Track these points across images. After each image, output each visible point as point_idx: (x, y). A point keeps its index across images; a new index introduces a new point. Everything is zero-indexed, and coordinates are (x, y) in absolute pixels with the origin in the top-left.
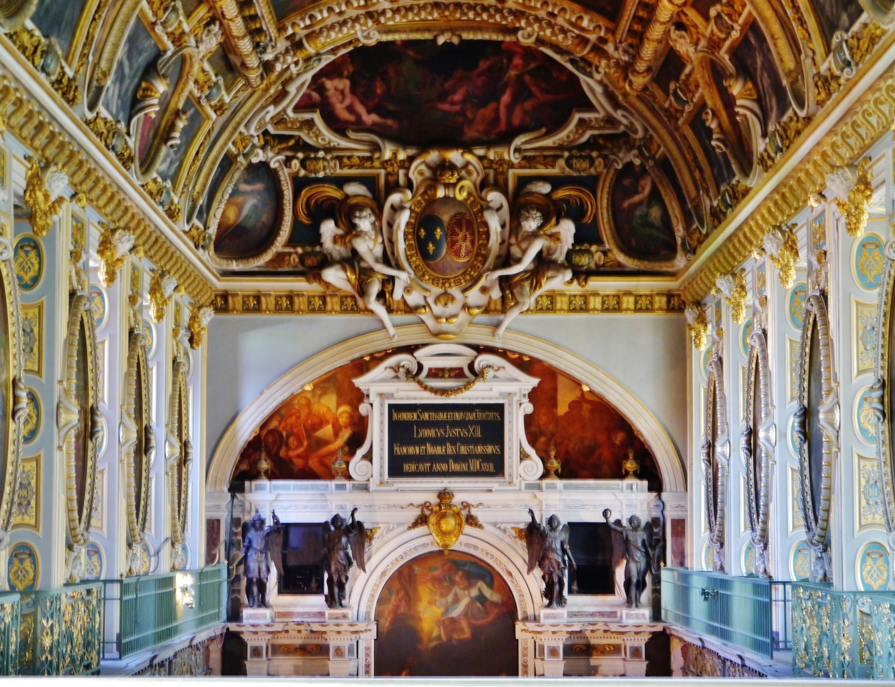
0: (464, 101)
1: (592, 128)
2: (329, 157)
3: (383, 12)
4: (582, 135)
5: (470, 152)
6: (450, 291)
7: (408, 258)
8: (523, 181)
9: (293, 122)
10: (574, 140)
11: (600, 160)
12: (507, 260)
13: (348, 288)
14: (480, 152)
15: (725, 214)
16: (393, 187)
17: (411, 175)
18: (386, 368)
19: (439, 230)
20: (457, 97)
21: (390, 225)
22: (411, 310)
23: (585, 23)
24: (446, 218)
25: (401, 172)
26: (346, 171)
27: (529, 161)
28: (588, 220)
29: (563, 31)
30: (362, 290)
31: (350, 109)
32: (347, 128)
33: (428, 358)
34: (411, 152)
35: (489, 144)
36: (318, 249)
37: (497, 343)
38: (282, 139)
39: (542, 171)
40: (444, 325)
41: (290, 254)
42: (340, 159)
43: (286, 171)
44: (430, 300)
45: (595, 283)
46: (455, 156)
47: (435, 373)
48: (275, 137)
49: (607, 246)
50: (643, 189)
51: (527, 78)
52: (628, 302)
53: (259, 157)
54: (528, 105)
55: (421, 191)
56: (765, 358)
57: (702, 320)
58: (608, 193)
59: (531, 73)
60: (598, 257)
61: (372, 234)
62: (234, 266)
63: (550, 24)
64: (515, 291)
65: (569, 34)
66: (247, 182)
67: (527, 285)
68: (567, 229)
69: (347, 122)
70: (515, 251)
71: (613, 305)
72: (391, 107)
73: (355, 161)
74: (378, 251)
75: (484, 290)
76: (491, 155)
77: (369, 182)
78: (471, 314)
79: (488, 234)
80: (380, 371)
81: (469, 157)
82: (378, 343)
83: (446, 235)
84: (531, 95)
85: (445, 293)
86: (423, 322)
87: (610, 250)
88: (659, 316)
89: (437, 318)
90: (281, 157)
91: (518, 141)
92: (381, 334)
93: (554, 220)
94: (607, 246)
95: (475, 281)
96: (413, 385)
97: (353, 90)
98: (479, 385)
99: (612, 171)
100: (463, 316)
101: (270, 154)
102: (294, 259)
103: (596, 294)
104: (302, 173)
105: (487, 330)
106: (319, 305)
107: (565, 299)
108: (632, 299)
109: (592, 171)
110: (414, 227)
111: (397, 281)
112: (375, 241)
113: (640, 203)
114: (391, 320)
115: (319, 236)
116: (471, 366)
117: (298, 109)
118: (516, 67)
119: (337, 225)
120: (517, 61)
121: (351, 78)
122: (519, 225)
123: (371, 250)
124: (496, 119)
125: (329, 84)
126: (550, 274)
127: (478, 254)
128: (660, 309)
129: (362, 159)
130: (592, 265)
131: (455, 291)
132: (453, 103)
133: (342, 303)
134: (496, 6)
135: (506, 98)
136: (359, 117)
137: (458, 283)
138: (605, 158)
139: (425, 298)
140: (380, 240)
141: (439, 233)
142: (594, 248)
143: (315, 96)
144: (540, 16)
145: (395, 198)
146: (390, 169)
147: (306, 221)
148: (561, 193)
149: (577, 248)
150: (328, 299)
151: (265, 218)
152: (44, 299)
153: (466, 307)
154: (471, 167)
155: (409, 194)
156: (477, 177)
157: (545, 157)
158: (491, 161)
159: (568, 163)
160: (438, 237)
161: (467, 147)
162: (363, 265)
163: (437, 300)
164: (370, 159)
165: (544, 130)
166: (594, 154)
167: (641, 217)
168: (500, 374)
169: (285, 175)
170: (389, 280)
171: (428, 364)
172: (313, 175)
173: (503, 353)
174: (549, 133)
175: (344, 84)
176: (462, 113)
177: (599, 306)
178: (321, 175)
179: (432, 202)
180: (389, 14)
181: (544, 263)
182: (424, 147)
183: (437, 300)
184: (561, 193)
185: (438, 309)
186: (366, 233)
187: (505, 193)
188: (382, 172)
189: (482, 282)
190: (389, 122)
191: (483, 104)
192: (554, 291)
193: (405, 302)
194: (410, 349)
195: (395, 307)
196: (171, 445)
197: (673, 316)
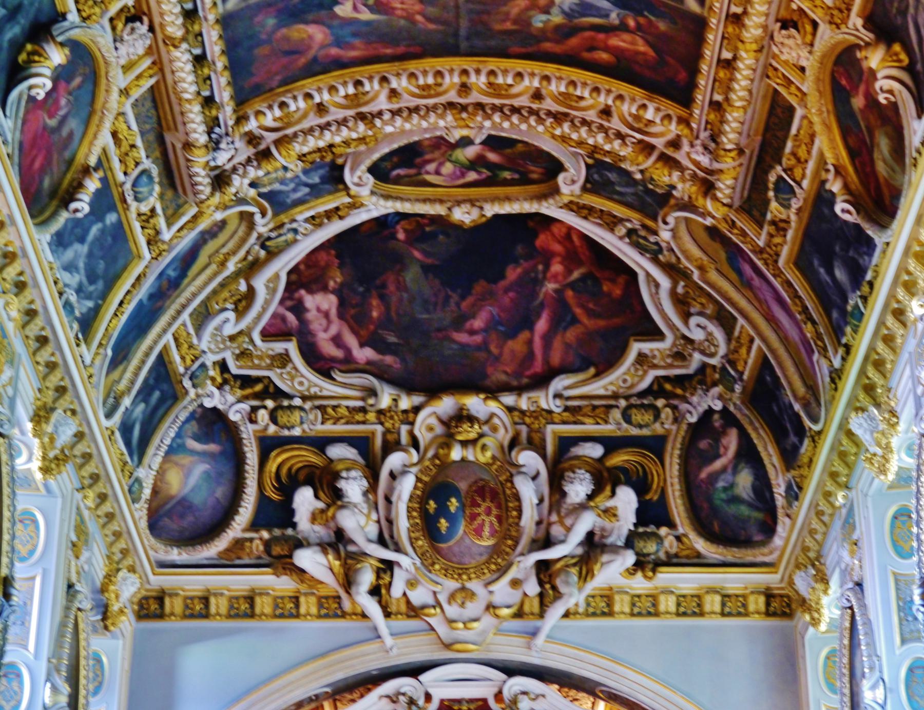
0: (485, 330)
1: (655, 367)
2: (308, 405)
3: (380, 114)
4: (642, 378)
5: (496, 399)
6: (469, 585)
8: (566, 443)
9: (260, 358)
10: (632, 386)
11: (668, 410)
12: (547, 542)
13: (331, 583)
14: (509, 399)
15: (870, 245)
16: (391, 446)
17: (417, 432)
18: (381, 697)
19: (454, 500)
20: (478, 323)
21: (388, 500)
22: (414, 611)
23: (649, 114)
25: (404, 429)
26: (329, 428)
27: (574, 413)
28: (653, 496)
29: (620, 136)
30: (348, 582)
31: (337, 340)
32: (332, 368)
34: (417, 399)
35: (519, 390)
36: (290, 532)
38: (246, 381)
39: (589, 427)
40: (462, 634)
41: (251, 540)
42: (322, 408)
43: (251, 427)
44: (442, 598)
45: (667, 577)
46: (475, 403)
48: (236, 377)
49: (681, 530)
50: (726, 449)
51: (570, 293)
52: (713, 603)
53: (215, 399)
54: (571, 334)
55: (430, 454)
57: (823, 579)
58: (680, 457)
59: (572, 285)
60: (670, 544)
61: (365, 508)
62: (175, 555)
63: (601, 128)
64: (558, 582)
65: (628, 141)
66: (197, 438)
67: (574, 571)
69: (333, 359)
70: (557, 531)
72: (392, 339)
73: (343, 411)
74: (372, 530)
75: (515, 583)
77: (361, 443)
78: (497, 616)
79: (520, 510)
81: (493, 406)
83: (463, 507)
84: (575, 321)
85: (463, 589)
86: (433, 629)
87: (685, 535)
88: (757, 622)
89: (451, 621)
90: (245, 407)
91: (559, 383)
92: (374, 646)
93: (608, 489)
94: (681, 530)
95: (502, 571)
97: (341, 316)
99: (684, 427)
100: (488, 621)
101: (231, 399)
103: (668, 592)
104: (272, 429)
105: (520, 641)
107: (627, 599)
108: (718, 598)
109: (658, 429)
110: (420, 500)
111: (396, 570)
112: (368, 516)
113: (724, 470)
114: (388, 627)
115: (292, 512)
116: (499, 696)
117: (267, 335)
118: (555, 277)
119: (317, 496)
120: (557, 267)
121: (338, 292)
122: (564, 494)
123: (362, 528)
124: (530, 356)
125: (312, 301)
126: (605, 558)
127: (507, 536)
128: (758, 613)
130: (662, 555)
131: (475, 585)
132: (472, 332)
133: (320, 606)
134: (530, 108)
135: (542, 325)
136: (348, 351)
137: (479, 574)
138: (674, 408)
139: (435, 593)
140: (374, 516)
141: (453, 504)
142: (663, 531)
143: (291, 317)
144: (588, 118)
145: (395, 460)
146: (388, 425)
147: (275, 497)
148: (619, 459)
149: (641, 530)
150: (302, 600)
151: (221, 492)
153: (491, 607)
154: (496, 421)
155: (415, 456)
156: (504, 436)
157: (595, 408)
158: (523, 413)
159: (627, 418)
160: (453, 509)
161: (492, 392)
162: (351, 548)
163: (452, 597)
164: (363, 410)
165: (592, 371)
166: (660, 403)
167: (725, 489)
169: (248, 433)
170: (388, 566)
172: (286, 433)
174: (598, 375)
175: (329, 302)
177: (673, 608)
178: (297, 432)
179: (444, 465)
180: (387, 116)
182: (433, 392)
184: (619, 459)
185: (452, 611)
186: (355, 506)
187: (544, 456)
188: (379, 429)
190: (389, 359)
191: (512, 334)
192: (611, 589)
193: (408, 602)
194: (415, 671)
195: (393, 608)
196: (55, 689)
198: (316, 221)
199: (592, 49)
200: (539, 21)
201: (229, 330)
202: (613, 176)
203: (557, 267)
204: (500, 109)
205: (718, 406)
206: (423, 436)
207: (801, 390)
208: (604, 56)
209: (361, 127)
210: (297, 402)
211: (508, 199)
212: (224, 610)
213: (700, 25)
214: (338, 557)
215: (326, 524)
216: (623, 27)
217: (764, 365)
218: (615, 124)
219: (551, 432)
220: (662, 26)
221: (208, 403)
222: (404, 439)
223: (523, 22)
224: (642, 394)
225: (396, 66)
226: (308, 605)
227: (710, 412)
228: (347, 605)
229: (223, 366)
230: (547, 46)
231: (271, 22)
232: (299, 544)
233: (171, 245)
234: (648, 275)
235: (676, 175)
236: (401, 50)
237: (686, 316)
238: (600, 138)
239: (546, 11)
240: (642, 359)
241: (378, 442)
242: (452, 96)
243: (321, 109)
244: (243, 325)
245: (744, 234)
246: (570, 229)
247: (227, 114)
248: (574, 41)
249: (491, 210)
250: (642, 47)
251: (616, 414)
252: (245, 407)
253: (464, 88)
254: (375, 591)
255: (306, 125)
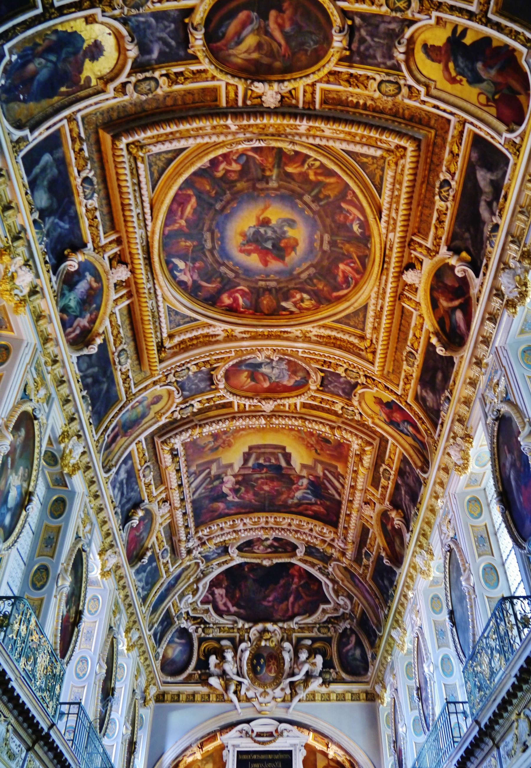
0: (273, 601)
7: (248, 674)
8: (299, 640)
12: (293, 674)
14: (280, 624)
15: (395, 573)
16: (242, 641)
20: (271, 599)
21: (240, 660)
22: (248, 700)
23: (325, 531)
24: (265, 655)
26: (222, 634)
27: (302, 629)
28: (328, 658)
29: (316, 537)
30: (226, 689)
31: (225, 604)
33: (257, 726)
34: (251, 624)
35: (284, 621)
37: (289, 717)
38: (195, 618)
39: (307, 634)
40: (264, 707)
42: (220, 628)
44: (258, 695)
46: (270, 626)
47: (259, 735)
51: (300, 589)
52: (348, 696)
54: (301, 602)
56: (422, 634)
57: (384, 687)
59: (301, 586)
60: (334, 675)
62: (169, 679)
64: (297, 689)
66: (178, 638)
67: (302, 685)
68: (319, 660)
69: (223, 611)
70: (296, 670)
71: (341, 698)
72: (243, 604)
74: (235, 670)
75: (282, 689)
76: (285, 626)
77: (232, 640)
80: (234, 732)
81: (275, 627)
82: (233, 718)
83: (265, 662)
84: (302, 598)
88: (362, 703)
89: (261, 703)
90: (194, 627)
91: (297, 619)
92: (234, 712)
95: (278, 685)
96: (249, 740)
97: (227, 596)
98: (280, 740)
100: (273, 703)
101: (190, 624)
102: (197, 676)
103: (334, 692)
104: (203, 635)
105: (284, 710)
106: (206, 699)
110: (251, 660)
113: (351, 649)
115: (208, 664)
116: (276, 731)
117: (202, 603)
120: (296, 580)
122: (299, 658)
124: (288, 609)
126: (312, 680)
129: (229, 628)
131: (269, 690)
132: (269, 602)
133: (217, 698)
135: (291, 599)
136: (228, 608)
138: (335, 628)
142: (332, 670)
143: (210, 597)
145: (243, 646)
147: (203, 658)
148: (317, 645)
151: (185, 657)
152: (63, 524)
153: (274, 698)
156: (279, 637)
159: (319, 631)
161: (275, 622)
163: (261, 695)
164: (233, 628)
166: (330, 626)
168: (290, 734)
169: (195, 636)
170: (240, 683)
171: (257, 730)
173: (292, 723)
174: (310, 616)
175: (222, 591)
176: (273, 606)
178: (211, 636)
179: (259, 647)
181: (309, 676)
182: (256, 622)
183: (261, 695)
184: (317, 645)
185: (261, 699)
187: (292, 643)
189: (282, 686)
190: (242, 611)
191: (281, 602)
197: (369, 703)
198: (219, 565)
199: (306, 510)
200: (290, 502)
201: (190, 601)
202: (314, 550)
203: (296, 580)
204: (278, 529)
205: (349, 627)
206: (252, 637)
207: (375, 621)
208: (310, 512)
209: (234, 535)
210: (211, 625)
211: (280, 557)
212: (184, 699)
213: (340, 503)
214: (223, 680)
215: (220, 668)
216: (316, 504)
217: (363, 613)
218: (314, 534)
219: (294, 635)
220: (328, 503)
221: (182, 626)
222: (246, 638)
223: (285, 502)
224: (324, 623)
225: (245, 516)
226: (213, 697)
227: (346, 629)
228: (226, 697)
229: (188, 613)
230: (293, 509)
231: (207, 502)
232: (211, 675)
233: (173, 573)
234: (325, 583)
235: (333, 550)
236: (247, 510)
237: (338, 596)
238: (309, 538)
239: (292, 498)
240: (324, 611)
241: (238, 639)
242: (263, 525)
243: (222, 529)
244: (195, 599)
245: (355, 569)
246: (300, 567)
247: (192, 531)
248: (301, 508)
249: (275, 561)
250: (322, 510)
251: (316, 630)
252: (194, 627)
253: (267, 522)
254: (235, 692)
255: (217, 534)
